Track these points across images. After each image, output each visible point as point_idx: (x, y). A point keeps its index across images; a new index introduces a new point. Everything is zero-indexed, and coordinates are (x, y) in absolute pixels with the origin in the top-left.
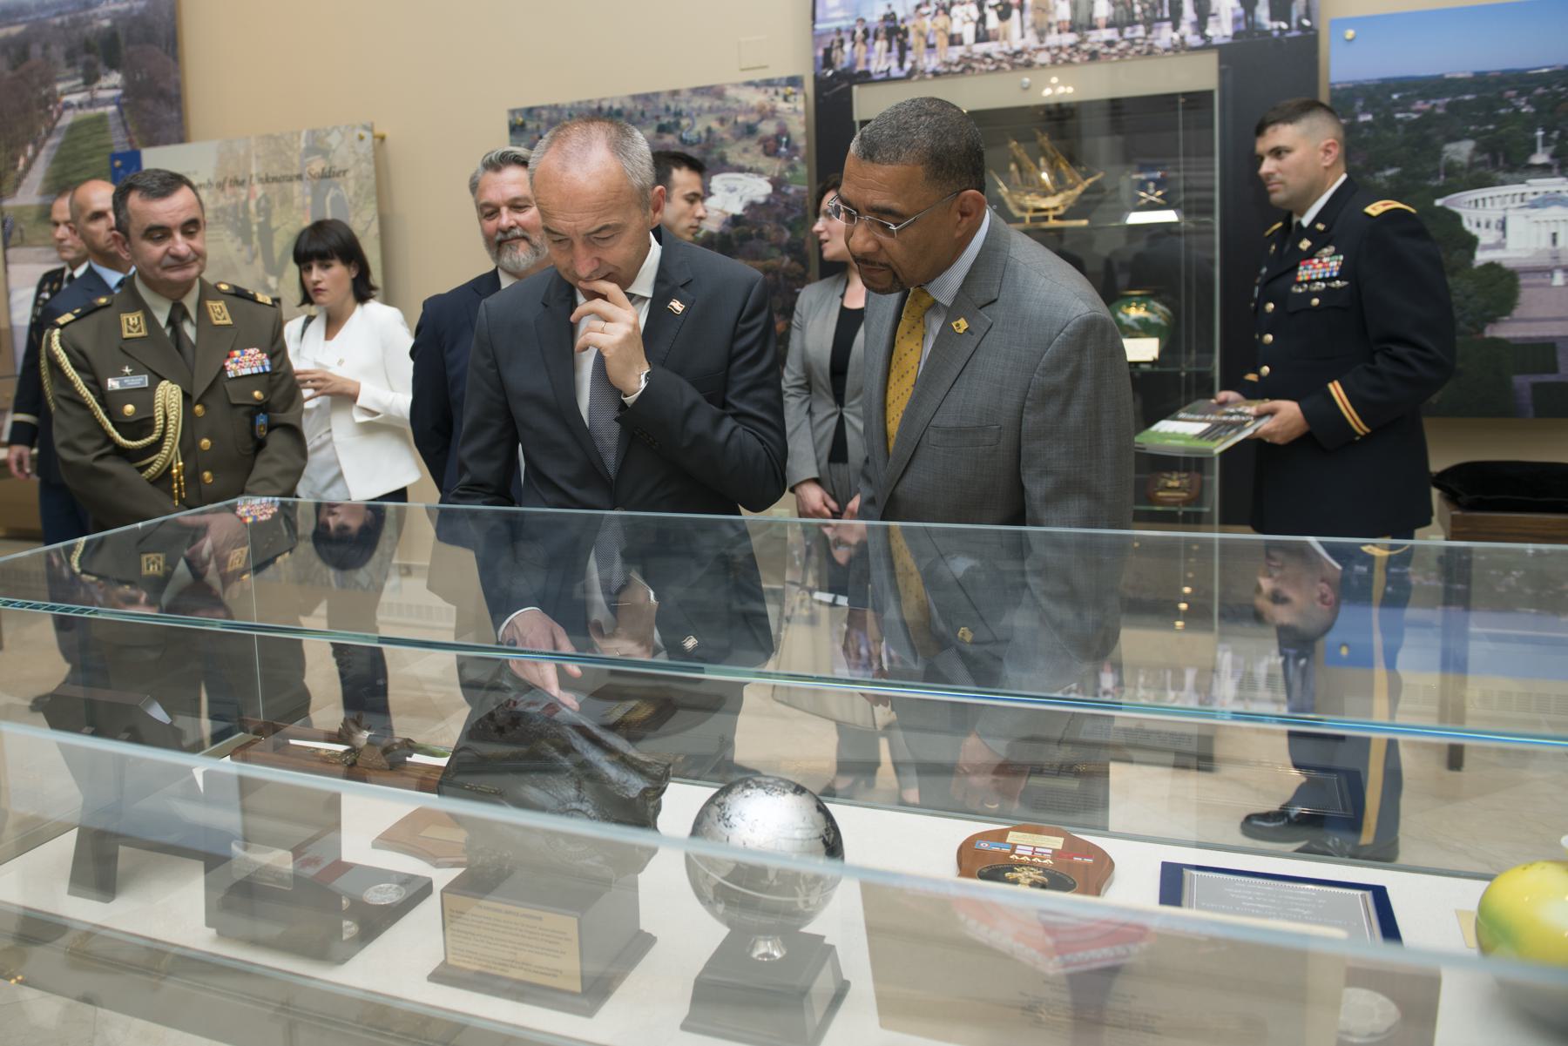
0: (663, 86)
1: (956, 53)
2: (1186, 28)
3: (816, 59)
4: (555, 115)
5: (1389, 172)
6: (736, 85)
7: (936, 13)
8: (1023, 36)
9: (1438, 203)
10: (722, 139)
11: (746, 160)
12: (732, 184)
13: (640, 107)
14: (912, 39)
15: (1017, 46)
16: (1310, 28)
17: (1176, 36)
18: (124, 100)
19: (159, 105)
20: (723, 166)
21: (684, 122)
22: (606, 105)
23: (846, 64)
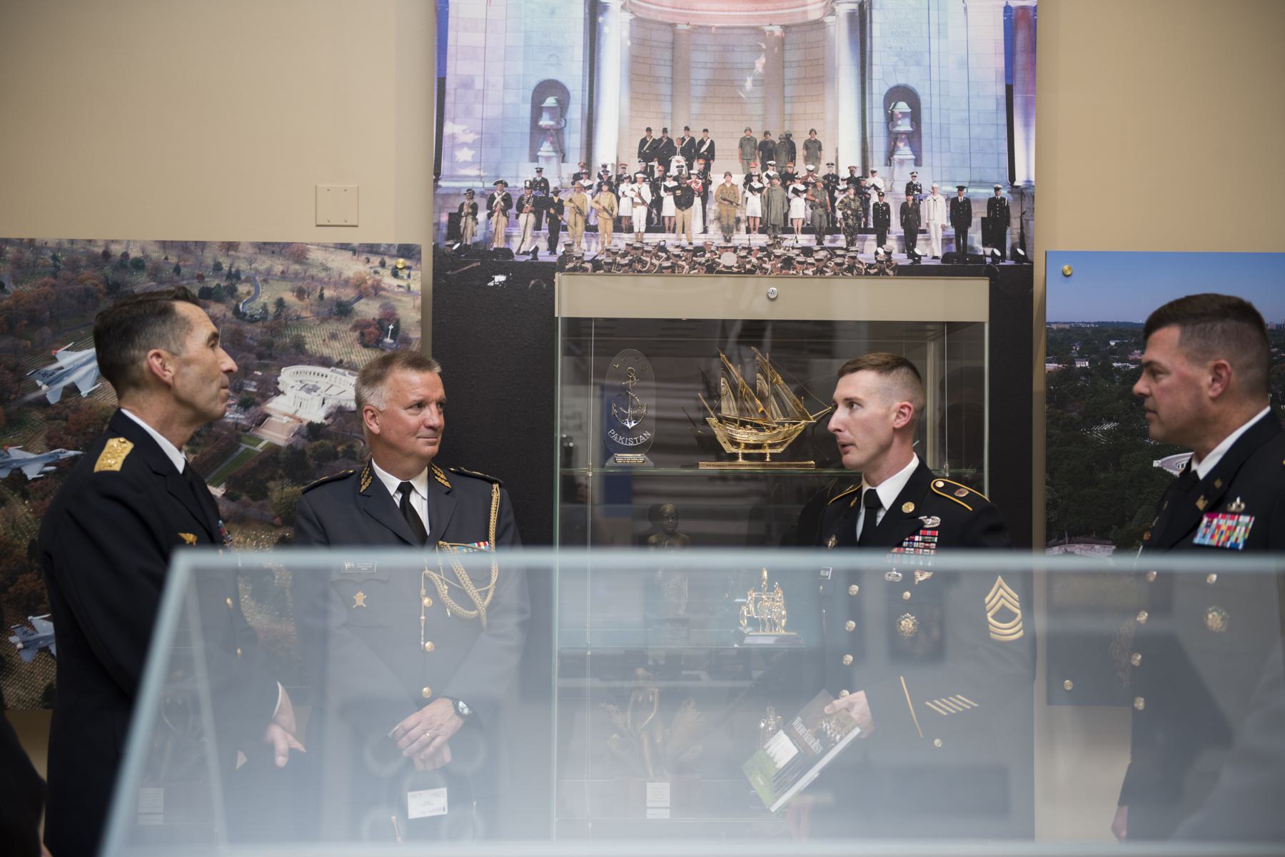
0: (215, 234)
1: (622, 241)
2: (892, 244)
4: (28, 254)
5: (1106, 427)
6: (325, 247)
7: (600, 189)
8: (705, 231)
9: (1156, 464)
10: (298, 318)
11: (334, 350)
12: (311, 381)
13: (173, 260)
14: (568, 216)
15: (699, 241)
16: (1025, 258)
17: (881, 251)
20: (299, 354)
21: (243, 288)
22: (117, 250)
23: (477, 239)
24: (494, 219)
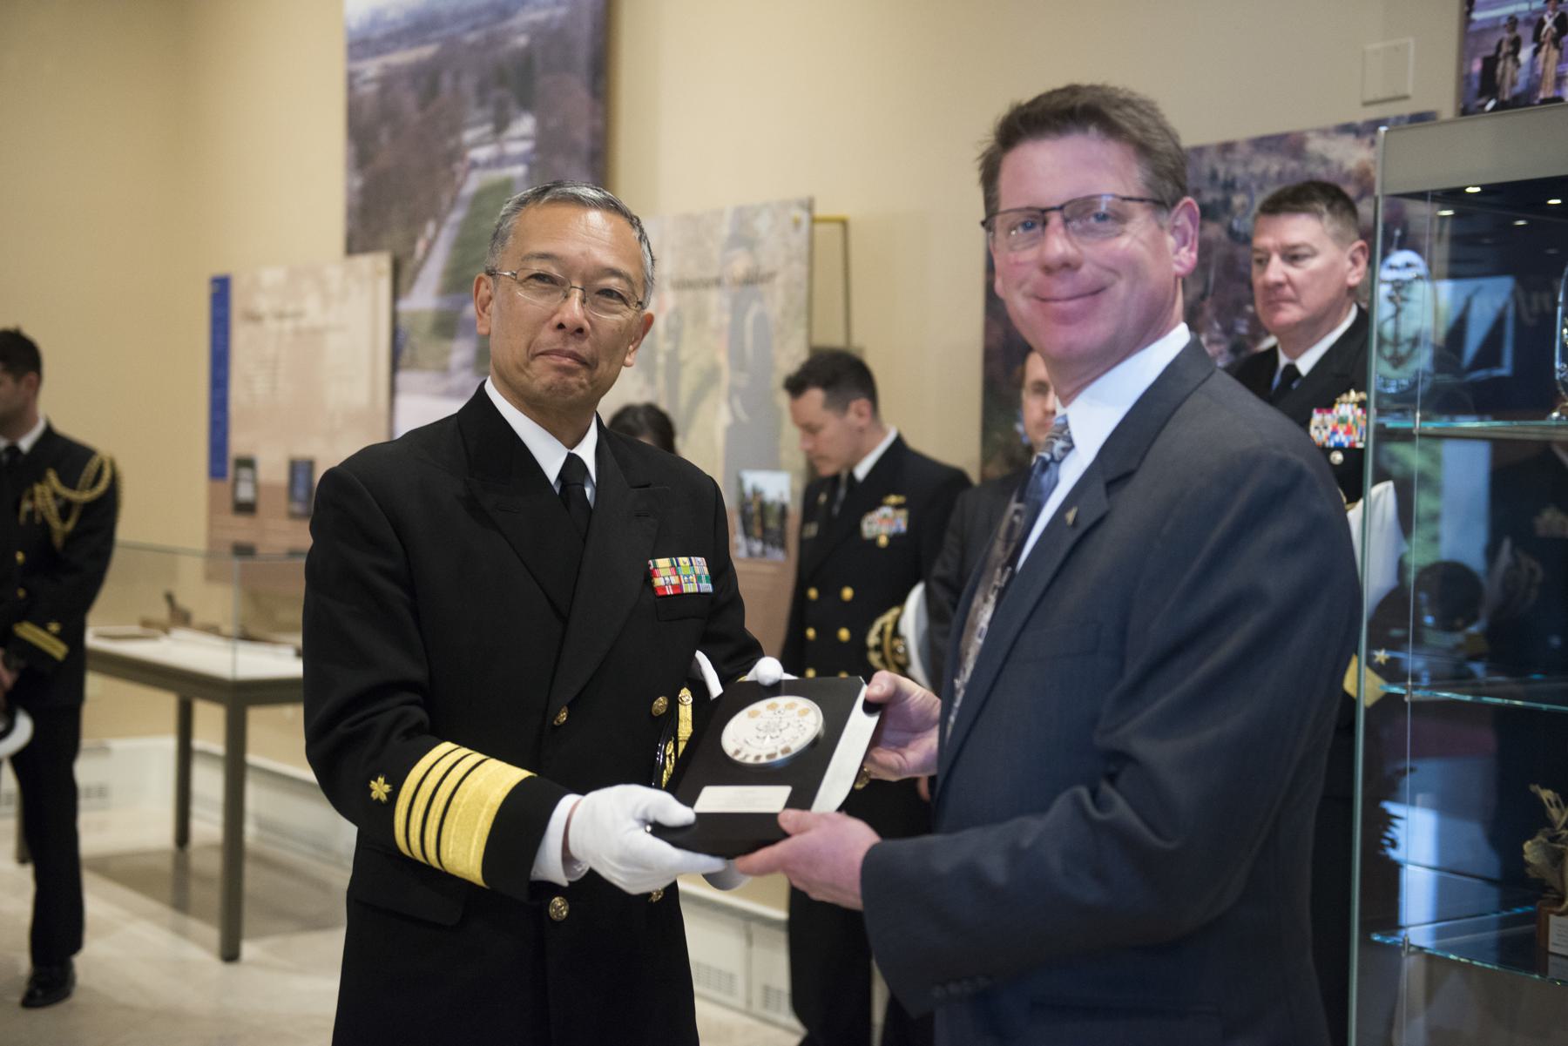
3: (1464, 79)
6: (1324, 132)
18: (534, 158)
19: (585, 156)
21: (1238, 200)
23: (1518, 89)
24: (1542, 55)
